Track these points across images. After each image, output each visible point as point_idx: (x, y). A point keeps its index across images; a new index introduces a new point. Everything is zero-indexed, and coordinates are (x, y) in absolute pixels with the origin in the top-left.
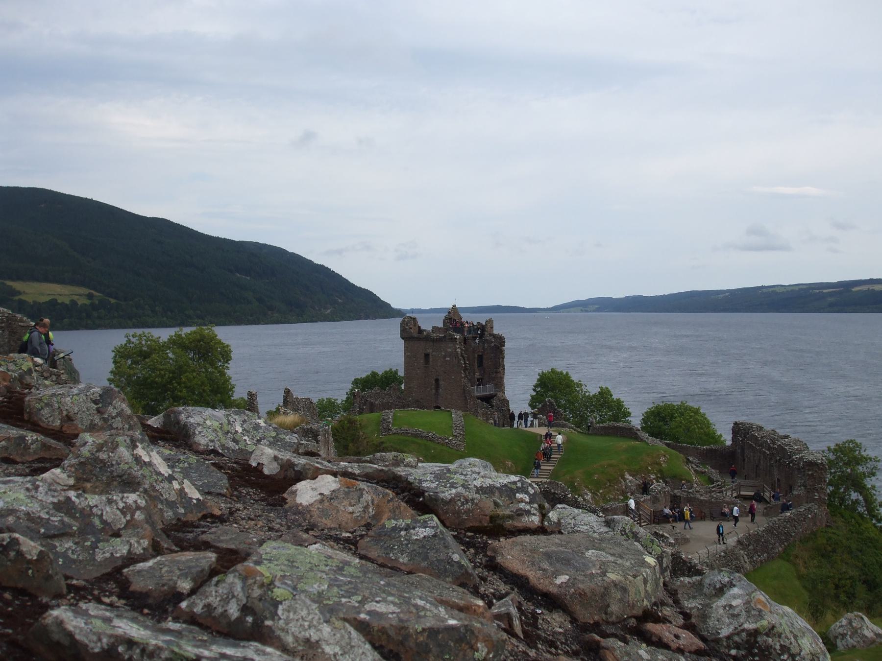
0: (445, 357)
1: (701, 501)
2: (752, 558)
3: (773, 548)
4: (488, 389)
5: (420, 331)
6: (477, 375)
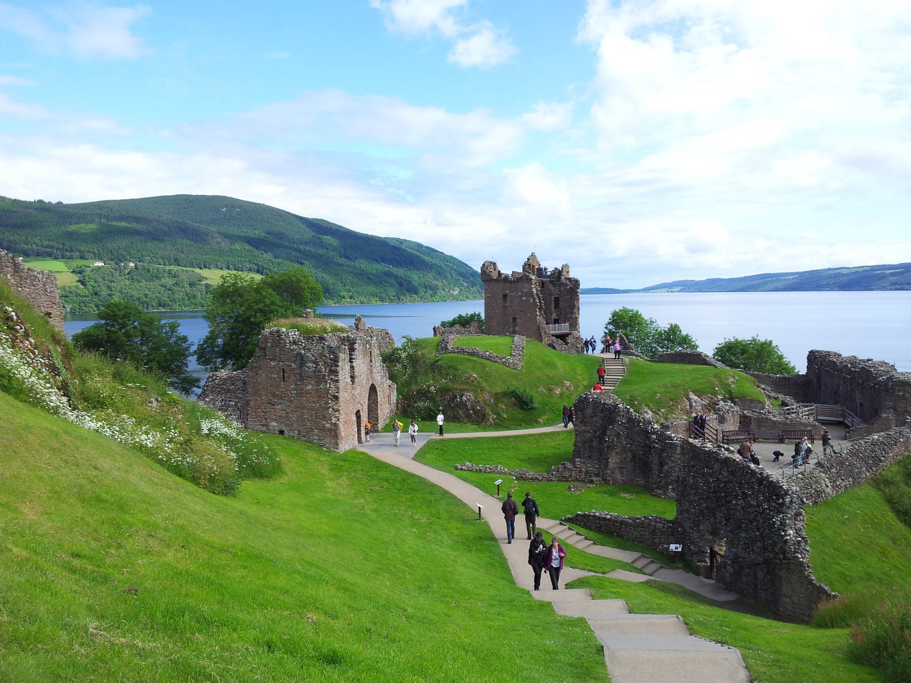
1: (774, 422)
2: (834, 482)
3: (859, 473)
4: (564, 328)
5: (500, 274)
6: (554, 316)
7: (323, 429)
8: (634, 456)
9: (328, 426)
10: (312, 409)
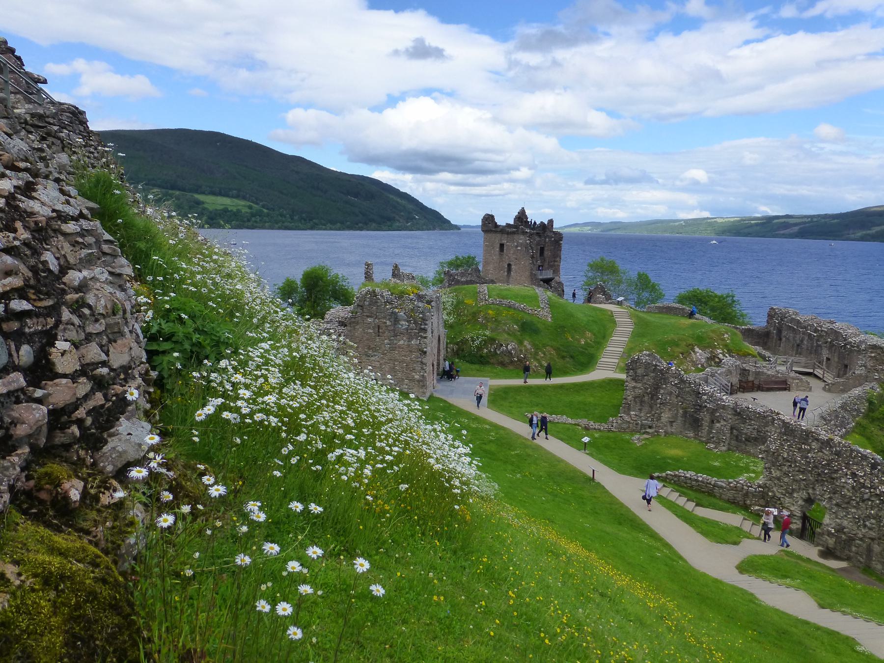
0: (517, 246)
7: (412, 380)
8: (685, 413)
9: (417, 377)
10: (403, 361)
